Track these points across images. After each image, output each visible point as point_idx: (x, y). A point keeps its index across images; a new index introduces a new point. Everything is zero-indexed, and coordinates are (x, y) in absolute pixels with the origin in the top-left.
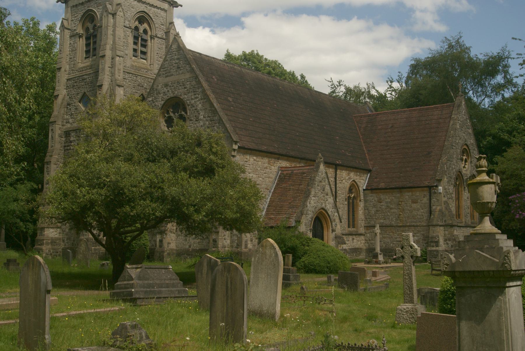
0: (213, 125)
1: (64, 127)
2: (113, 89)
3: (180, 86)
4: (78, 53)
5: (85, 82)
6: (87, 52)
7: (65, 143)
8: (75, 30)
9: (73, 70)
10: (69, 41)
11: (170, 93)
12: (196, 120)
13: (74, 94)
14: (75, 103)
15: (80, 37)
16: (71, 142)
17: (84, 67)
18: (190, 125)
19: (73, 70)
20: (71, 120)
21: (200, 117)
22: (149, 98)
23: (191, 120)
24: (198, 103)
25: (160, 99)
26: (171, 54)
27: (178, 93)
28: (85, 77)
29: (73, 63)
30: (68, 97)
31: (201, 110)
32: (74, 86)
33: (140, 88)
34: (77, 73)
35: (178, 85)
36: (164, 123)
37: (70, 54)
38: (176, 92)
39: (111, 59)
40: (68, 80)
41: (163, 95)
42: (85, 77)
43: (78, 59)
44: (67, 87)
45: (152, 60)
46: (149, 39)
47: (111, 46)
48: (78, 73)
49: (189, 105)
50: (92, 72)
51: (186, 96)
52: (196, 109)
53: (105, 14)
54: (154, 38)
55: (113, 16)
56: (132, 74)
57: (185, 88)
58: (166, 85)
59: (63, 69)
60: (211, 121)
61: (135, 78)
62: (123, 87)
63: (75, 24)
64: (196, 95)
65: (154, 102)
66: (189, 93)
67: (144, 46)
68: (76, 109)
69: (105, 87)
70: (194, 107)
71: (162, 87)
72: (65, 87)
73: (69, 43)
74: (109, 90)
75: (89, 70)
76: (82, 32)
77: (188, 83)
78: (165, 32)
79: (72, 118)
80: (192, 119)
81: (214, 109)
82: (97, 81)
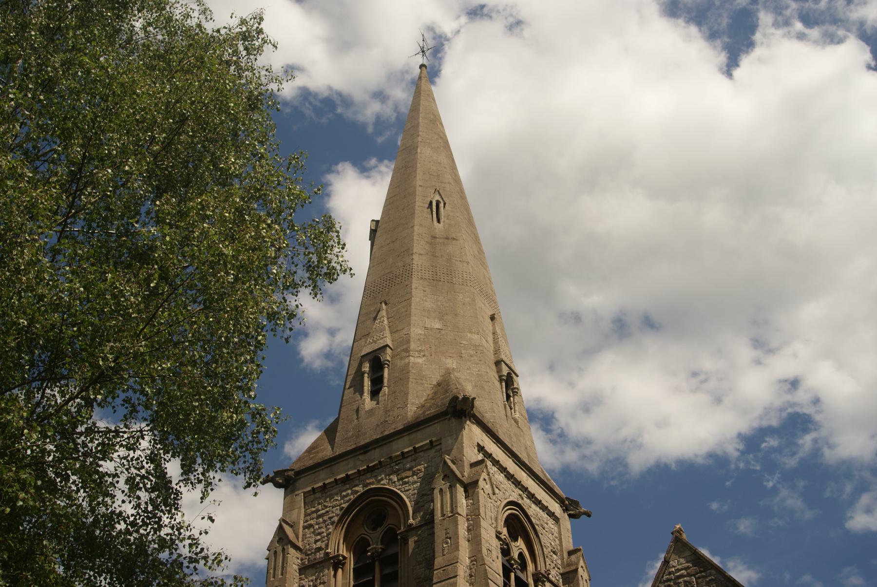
8: (319, 549)
10: (297, 580)
15: (338, 563)
47: (468, 572)
53: (440, 483)
54: (543, 582)
55: (466, 491)
63: (319, 534)
76: (343, 551)
78: (561, 574)
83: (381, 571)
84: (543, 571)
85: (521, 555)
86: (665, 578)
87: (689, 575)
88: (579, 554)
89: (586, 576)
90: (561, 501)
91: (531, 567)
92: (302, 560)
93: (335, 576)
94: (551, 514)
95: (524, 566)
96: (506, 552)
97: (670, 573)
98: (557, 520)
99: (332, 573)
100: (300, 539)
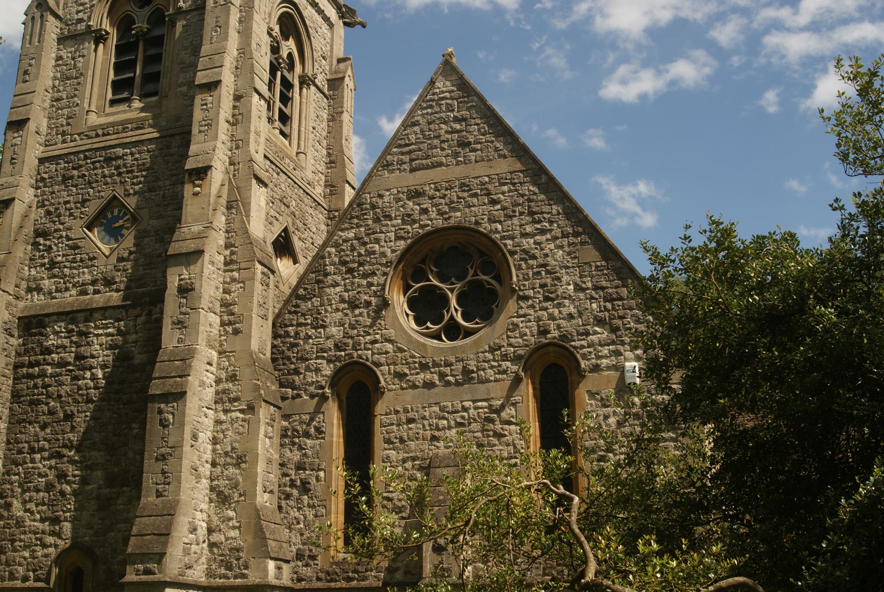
0: (621, 313)
1: (21, 304)
2: (238, 188)
3: (475, 195)
4: (89, 86)
5: (117, 168)
6: (117, 86)
7: (18, 354)
8: (80, 21)
9: (64, 134)
10: (54, 50)
11: (433, 215)
12: (547, 299)
13: (66, 203)
14: (70, 229)
15: (100, 38)
16: (48, 351)
17: (102, 127)
18: (521, 312)
19: (64, 134)
20: (46, 284)
21: (560, 291)
22: (342, 230)
23: (526, 298)
24: (552, 246)
25: (392, 235)
26: (431, 107)
27: (464, 215)
28: (120, 151)
29: (65, 111)
30: (42, 211)
31: (567, 267)
32: (72, 178)
33: (283, 207)
34: (80, 143)
35: (466, 194)
36: (406, 306)
37: (54, 86)
38: (458, 214)
39: (231, 97)
40: (42, 161)
41: (404, 222)
42: (120, 151)
43: (87, 101)
44: (40, 182)
45: (302, 143)
46: (296, 83)
47: (235, 63)
48: (89, 141)
49: (512, 253)
50: (156, 135)
51: (499, 227)
52: (544, 265)
54: (308, 85)
56: (272, 162)
57: (494, 202)
58: (415, 194)
59: (32, 126)
60: (609, 299)
61: (275, 175)
62: (266, 185)
64: (539, 222)
65: (365, 244)
66: (511, 217)
67: (285, 99)
68: (76, 247)
69: (217, 176)
70: (534, 257)
71: (398, 200)
72: (33, 182)
73: (54, 55)
74: (226, 187)
75: (130, 133)
76: (106, 25)
77: (505, 188)
78: (328, 80)
79: (54, 276)
80: (531, 293)
81: (619, 264)
82: (185, 156)
83: (145, 51)
84: (310, 75)
85: (290, 55)
86: (428, 98)
87: (452, 98)
88: (348, 62)
89: (351, 86)
90: (339, 8)
91: (298, 69)
92: (61, 29)
93: (96, 50)
94: (326, 19)
95: (291, 67)
96: (275, 50)
97: (434, 94)
98: (331, 25)
99: (93, 47)
100: (61, 7)
